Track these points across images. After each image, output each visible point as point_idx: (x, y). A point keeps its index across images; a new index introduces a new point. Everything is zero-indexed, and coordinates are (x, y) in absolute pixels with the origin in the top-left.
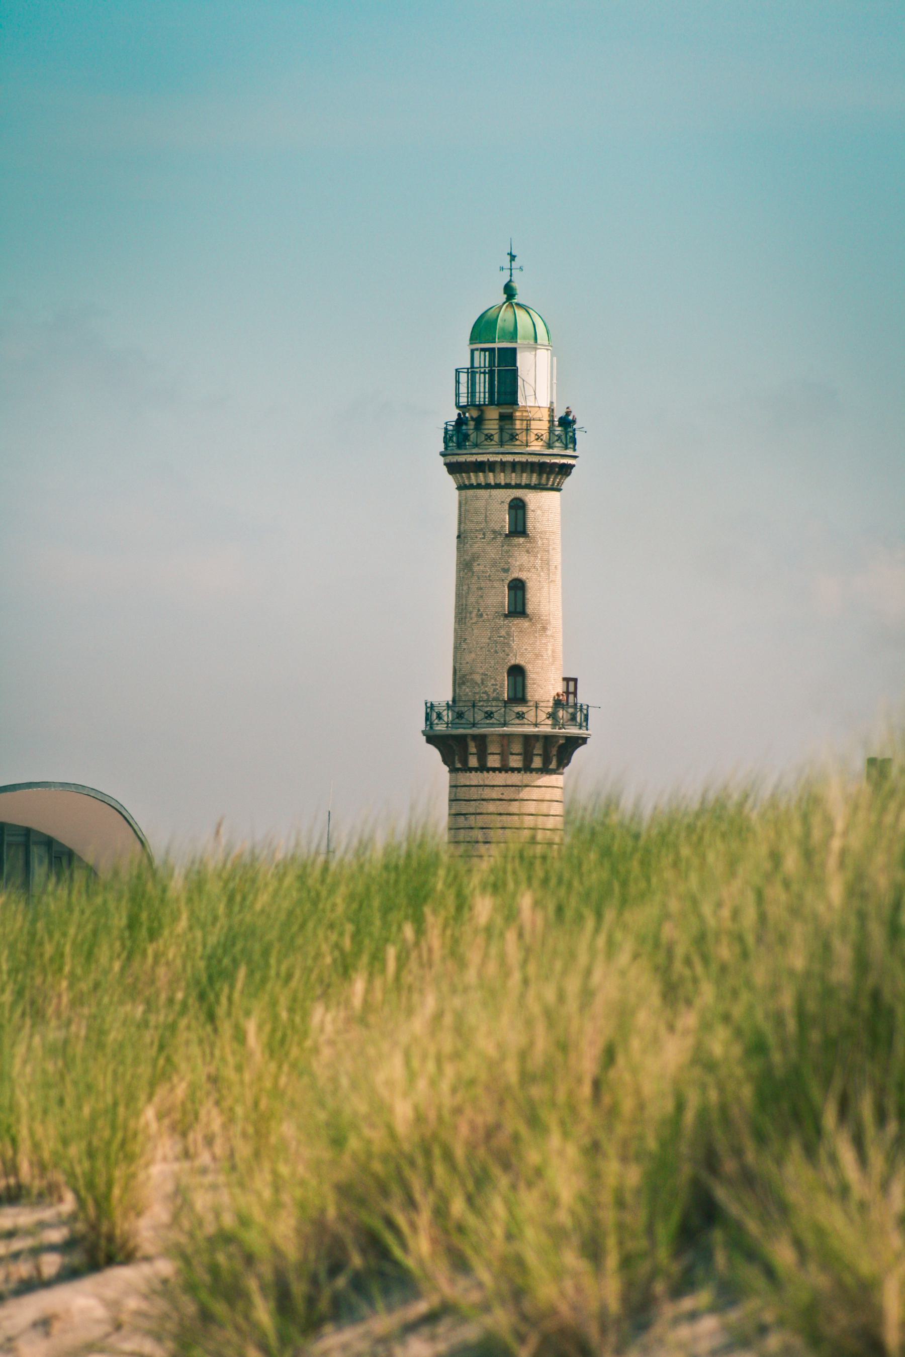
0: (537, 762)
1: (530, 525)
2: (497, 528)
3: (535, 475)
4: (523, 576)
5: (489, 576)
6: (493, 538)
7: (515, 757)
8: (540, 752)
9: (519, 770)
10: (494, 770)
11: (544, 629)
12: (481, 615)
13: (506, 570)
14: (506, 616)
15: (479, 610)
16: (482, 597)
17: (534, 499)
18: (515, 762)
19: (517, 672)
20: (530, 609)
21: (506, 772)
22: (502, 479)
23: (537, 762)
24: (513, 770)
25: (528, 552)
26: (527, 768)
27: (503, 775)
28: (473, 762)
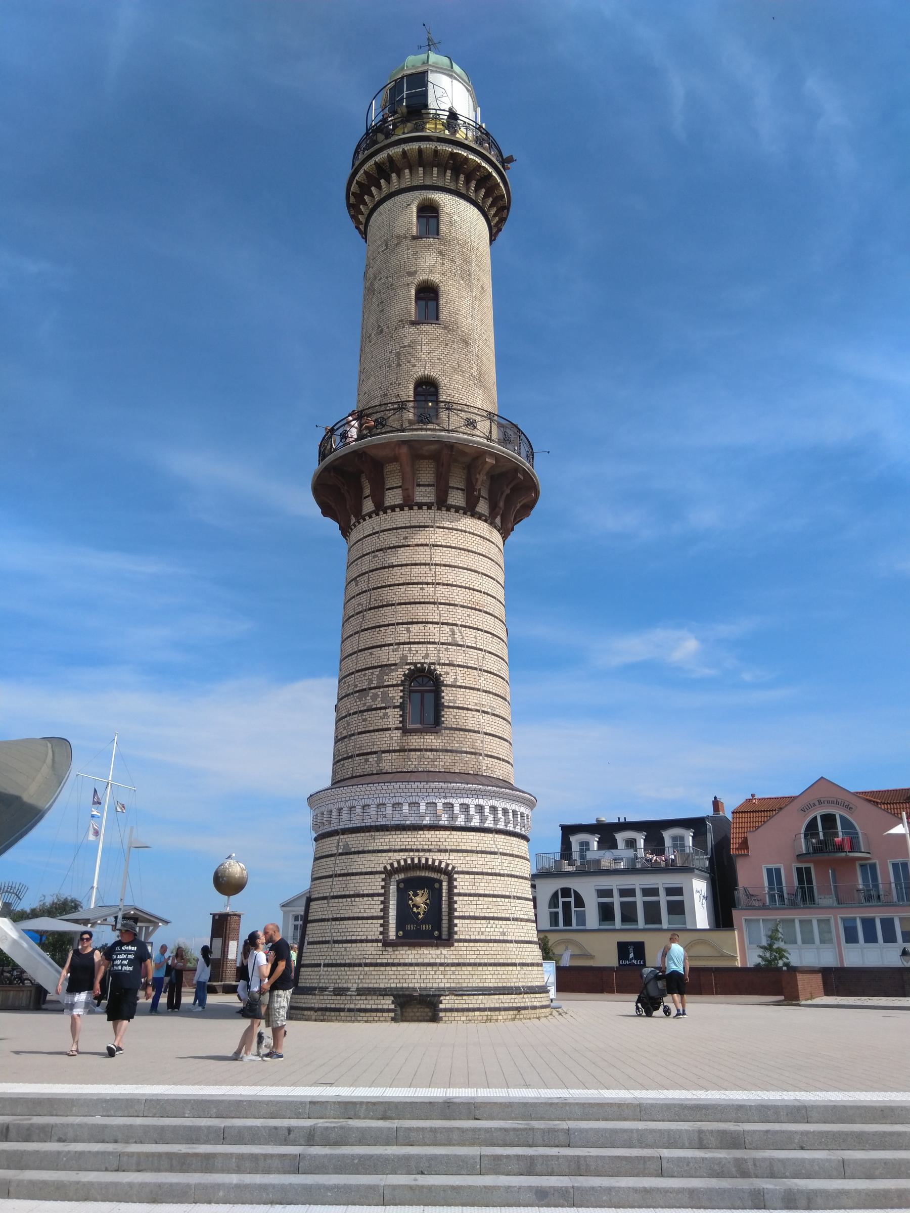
0: (457, 498)
1: (443, 228)
2: (401, 232)
3: (449, 173)
4: (436, 278)
5: (392, 285)
6: (397, 245)
7: (423, 489)
8: (462, 486)
9: (429, 506)
10: (393, 508)
11: (466, 343)
12: (382, 331)
13: (412, 274)
14: (413, 323)
15: (379, 326)
16: (382, 311)
17: (449, 204)
18: (424, 495)
19: (427, 388)
20: (444, 314)
21: (411, 508)
22: (407, 181)
23: (457, 498)
24: (420, 506)
25: (441, 253)
26: (442, 504)
27: (406, 512)
28: (368, 506)
